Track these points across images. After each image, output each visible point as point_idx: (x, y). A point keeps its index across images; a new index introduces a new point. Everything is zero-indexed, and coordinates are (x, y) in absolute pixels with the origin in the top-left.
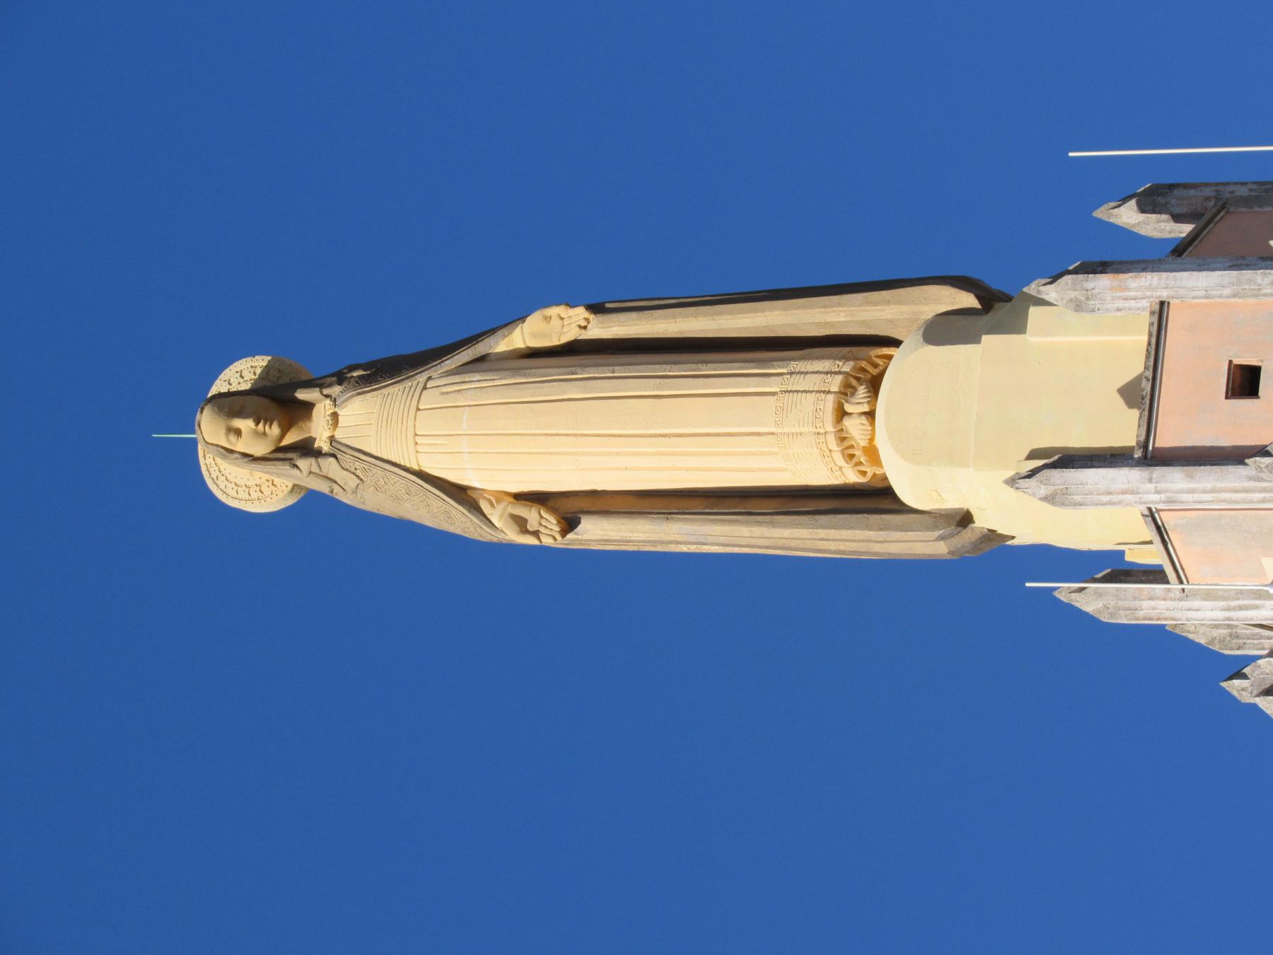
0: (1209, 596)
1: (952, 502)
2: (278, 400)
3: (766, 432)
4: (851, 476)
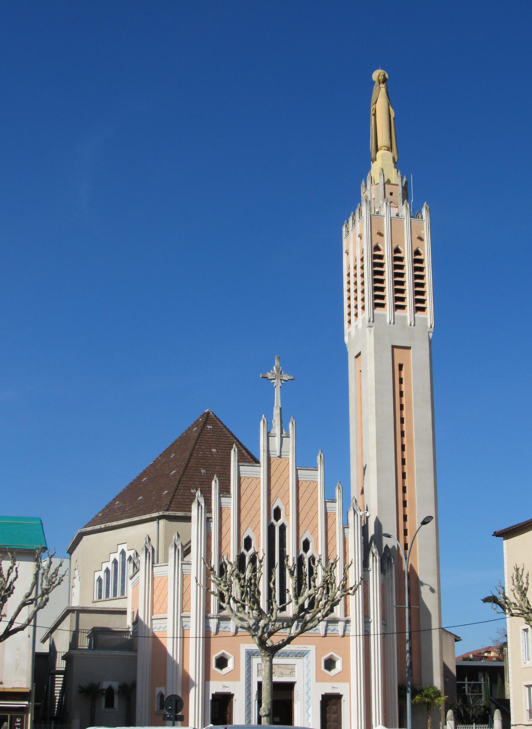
0: (371, 189)
1: (377, 159)
2: (385, 81)
3: (383, 139)
4: (379, 147)
